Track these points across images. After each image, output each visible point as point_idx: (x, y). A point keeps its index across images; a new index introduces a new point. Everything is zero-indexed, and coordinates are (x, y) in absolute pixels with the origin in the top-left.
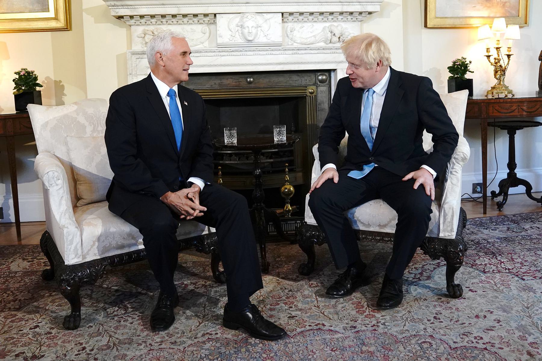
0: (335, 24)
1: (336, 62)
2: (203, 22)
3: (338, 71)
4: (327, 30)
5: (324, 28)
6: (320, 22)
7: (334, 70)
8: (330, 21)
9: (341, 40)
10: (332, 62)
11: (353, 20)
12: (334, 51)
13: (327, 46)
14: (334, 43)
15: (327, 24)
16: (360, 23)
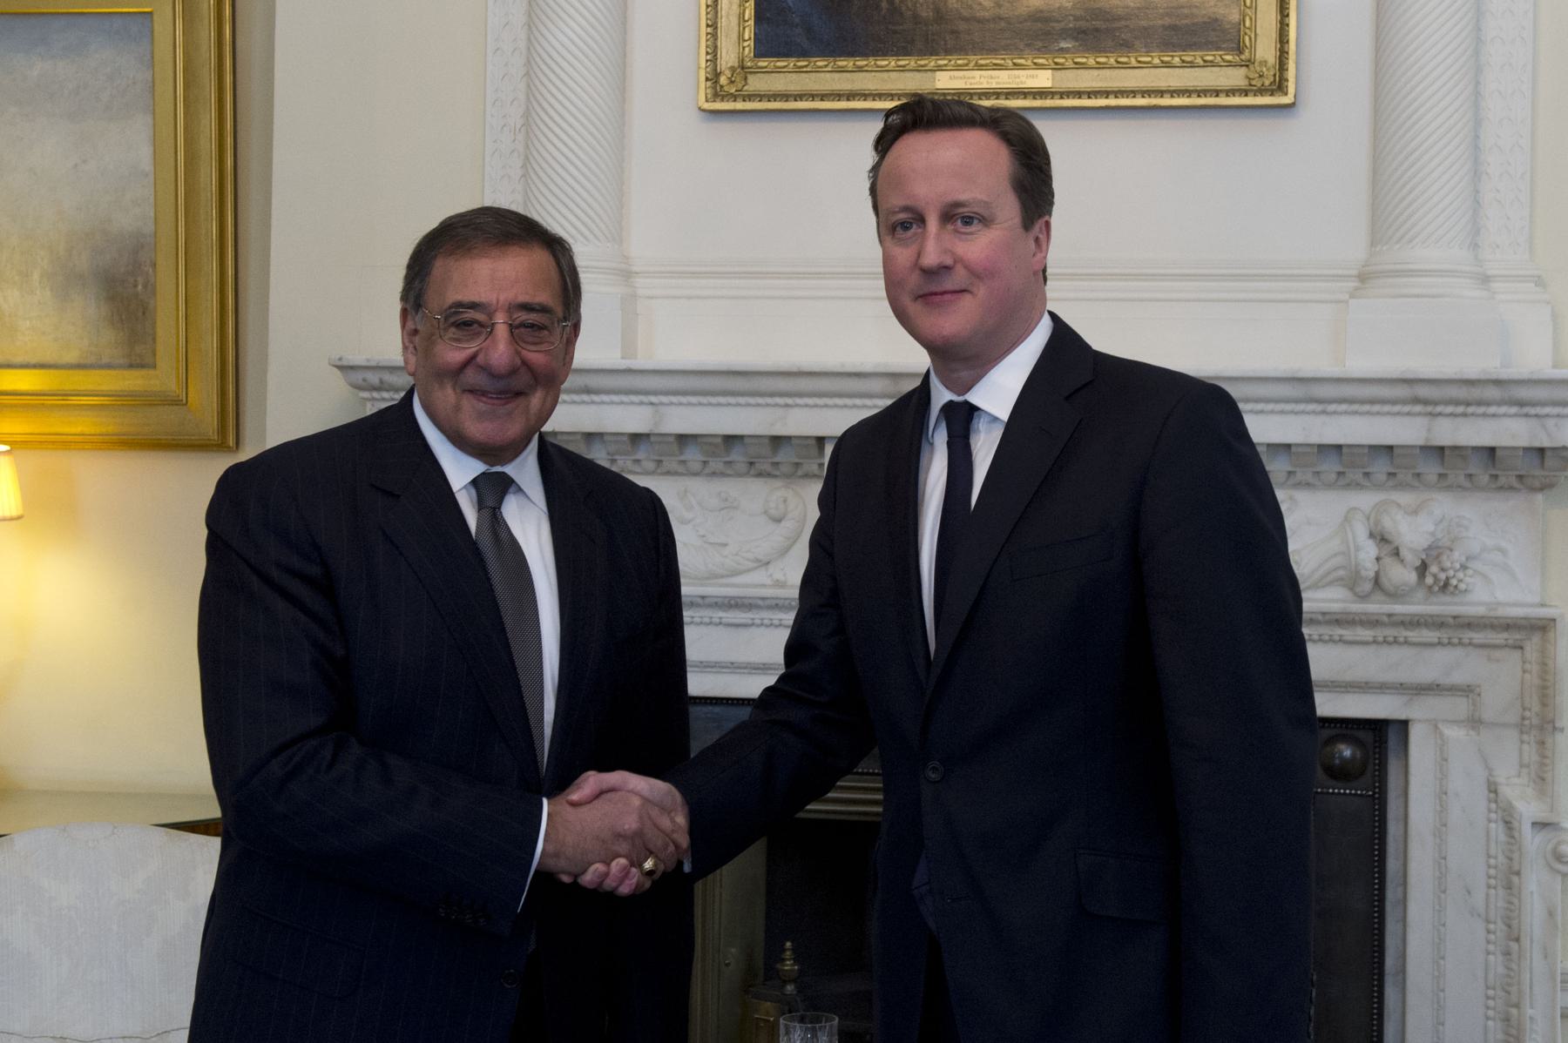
0: (1406, 498)
1: (1401, 688)
2: (767, 467)
3: (1416, 734)
4: (1361, 532)
5: (1347, 519)
6: (1330, 486)
7: (1404, 725)
8: (1379, 487)
9: (1429, 580)
10: (1382, 688)
11: (1502, 481)
12: (1390, 632)
13: (1357, 607)
14: (1395, 595)
15: (1365, 500)
16: (1540, 497)
